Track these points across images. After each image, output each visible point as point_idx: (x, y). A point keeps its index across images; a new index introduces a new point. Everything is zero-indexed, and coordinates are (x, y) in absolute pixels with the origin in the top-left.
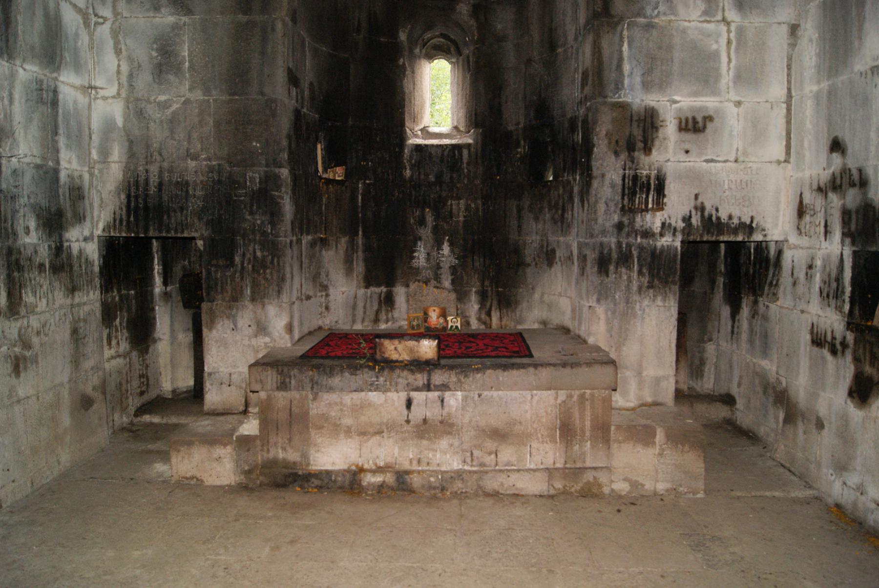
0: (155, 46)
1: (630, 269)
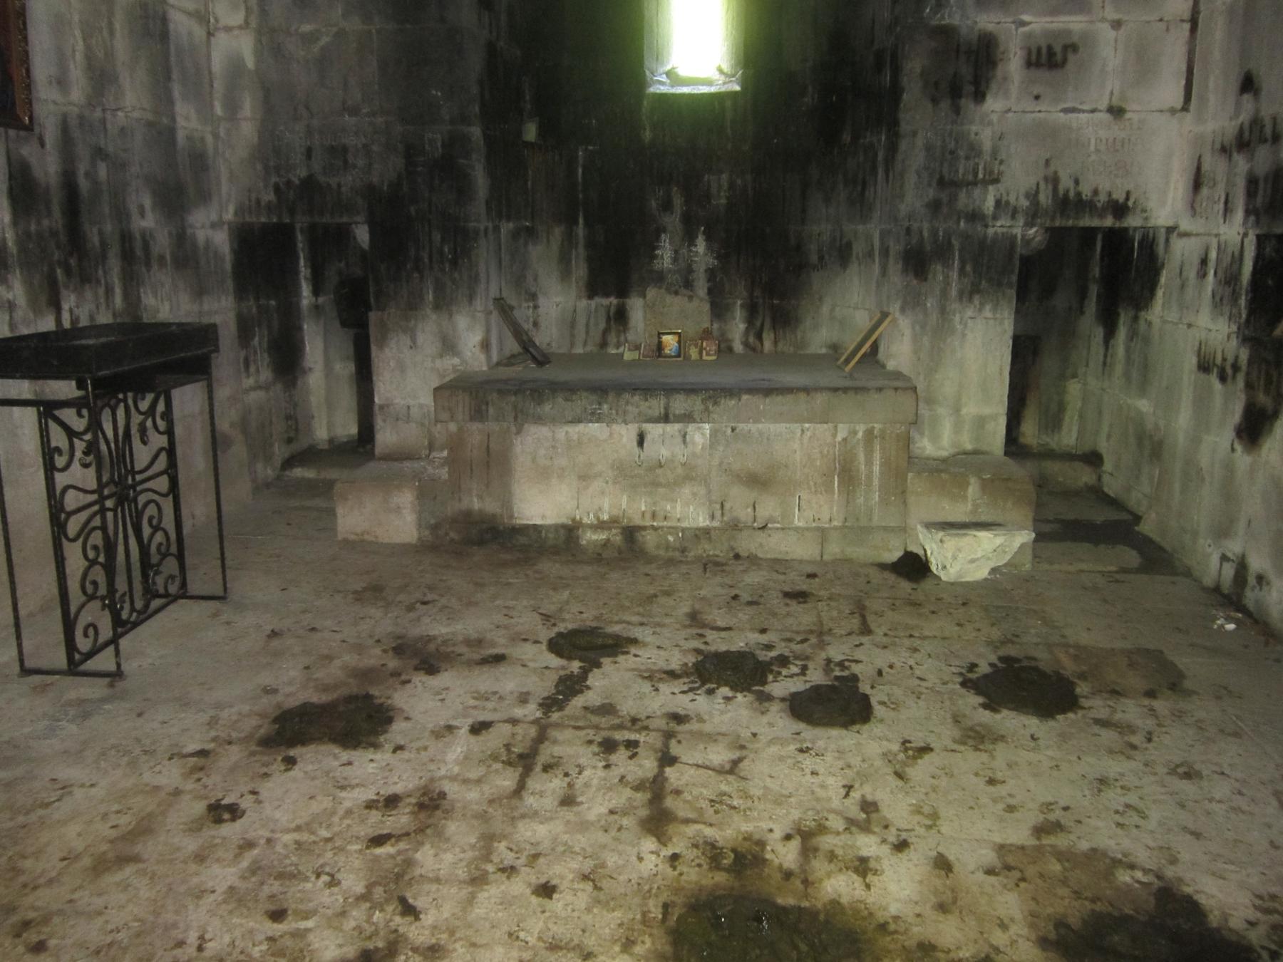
1: (947, 265)
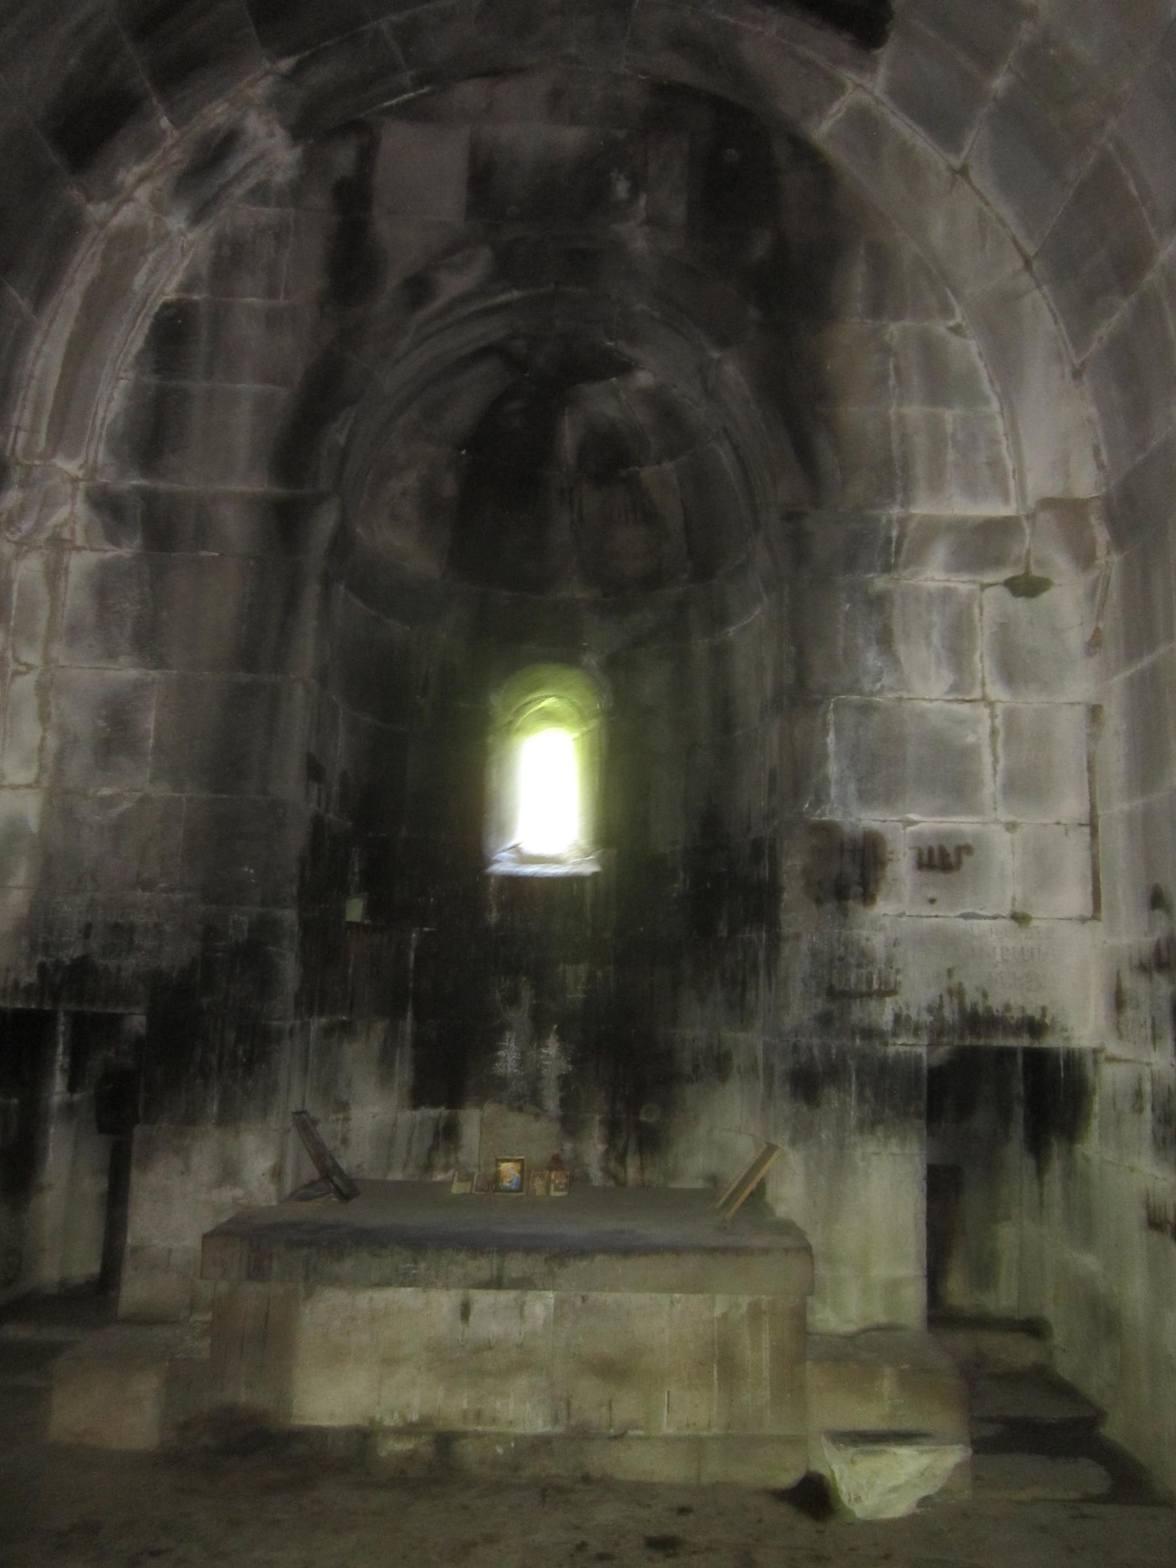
0: (104, 712)
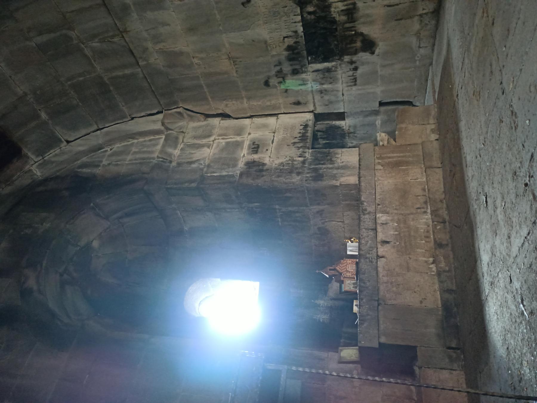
1: (321, 169)
